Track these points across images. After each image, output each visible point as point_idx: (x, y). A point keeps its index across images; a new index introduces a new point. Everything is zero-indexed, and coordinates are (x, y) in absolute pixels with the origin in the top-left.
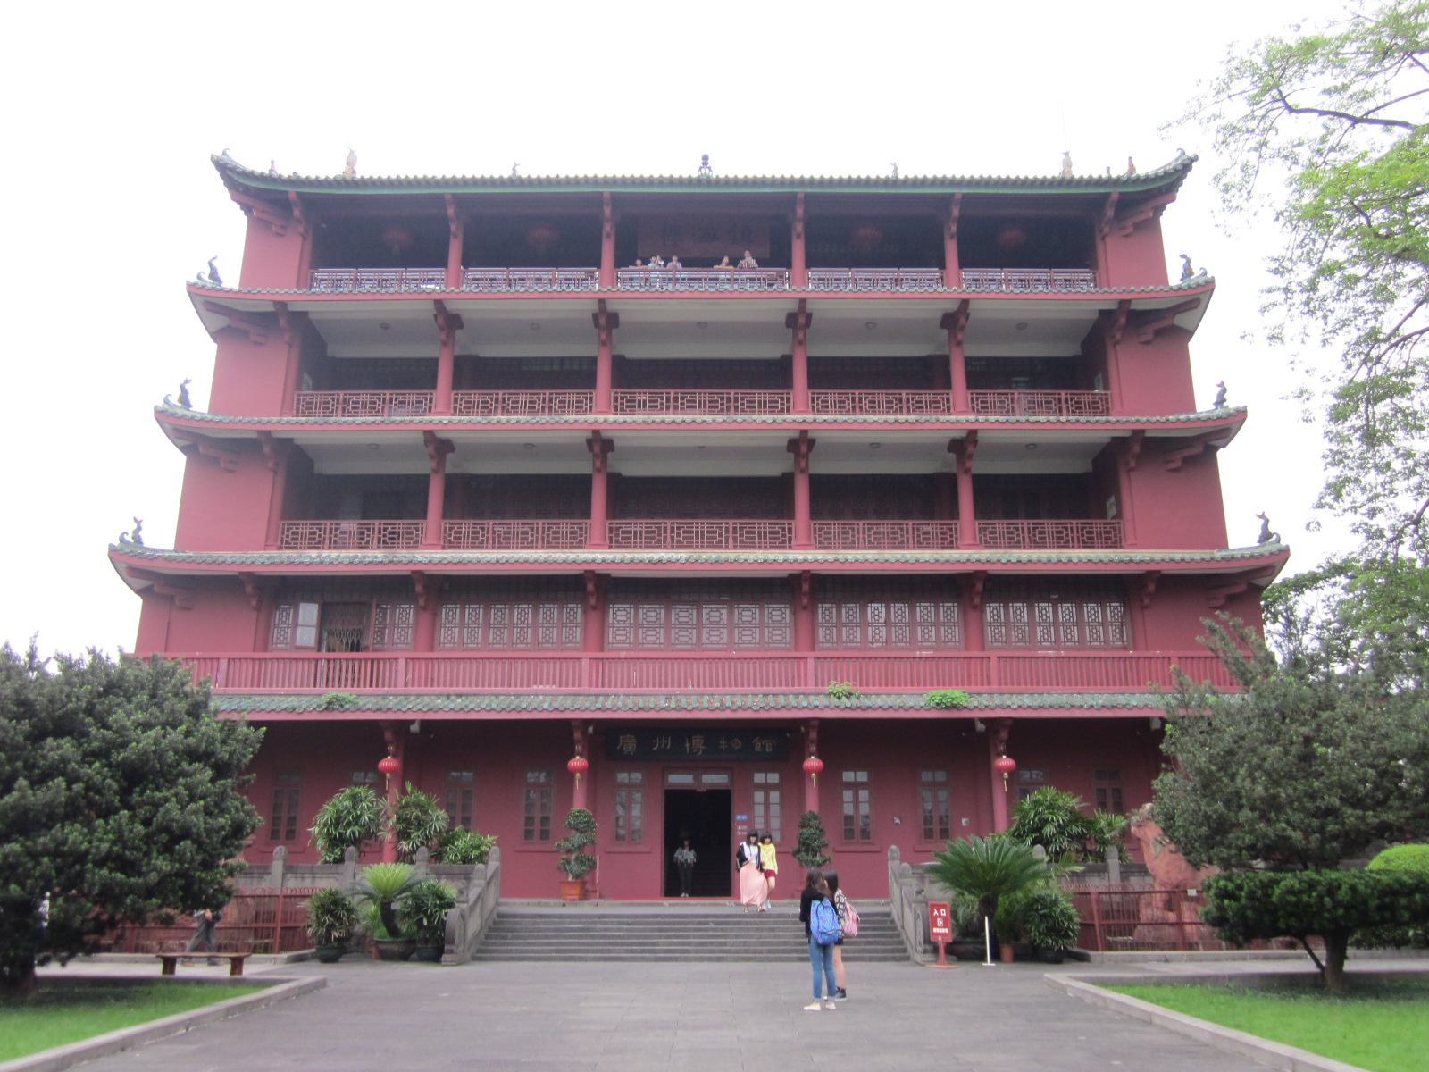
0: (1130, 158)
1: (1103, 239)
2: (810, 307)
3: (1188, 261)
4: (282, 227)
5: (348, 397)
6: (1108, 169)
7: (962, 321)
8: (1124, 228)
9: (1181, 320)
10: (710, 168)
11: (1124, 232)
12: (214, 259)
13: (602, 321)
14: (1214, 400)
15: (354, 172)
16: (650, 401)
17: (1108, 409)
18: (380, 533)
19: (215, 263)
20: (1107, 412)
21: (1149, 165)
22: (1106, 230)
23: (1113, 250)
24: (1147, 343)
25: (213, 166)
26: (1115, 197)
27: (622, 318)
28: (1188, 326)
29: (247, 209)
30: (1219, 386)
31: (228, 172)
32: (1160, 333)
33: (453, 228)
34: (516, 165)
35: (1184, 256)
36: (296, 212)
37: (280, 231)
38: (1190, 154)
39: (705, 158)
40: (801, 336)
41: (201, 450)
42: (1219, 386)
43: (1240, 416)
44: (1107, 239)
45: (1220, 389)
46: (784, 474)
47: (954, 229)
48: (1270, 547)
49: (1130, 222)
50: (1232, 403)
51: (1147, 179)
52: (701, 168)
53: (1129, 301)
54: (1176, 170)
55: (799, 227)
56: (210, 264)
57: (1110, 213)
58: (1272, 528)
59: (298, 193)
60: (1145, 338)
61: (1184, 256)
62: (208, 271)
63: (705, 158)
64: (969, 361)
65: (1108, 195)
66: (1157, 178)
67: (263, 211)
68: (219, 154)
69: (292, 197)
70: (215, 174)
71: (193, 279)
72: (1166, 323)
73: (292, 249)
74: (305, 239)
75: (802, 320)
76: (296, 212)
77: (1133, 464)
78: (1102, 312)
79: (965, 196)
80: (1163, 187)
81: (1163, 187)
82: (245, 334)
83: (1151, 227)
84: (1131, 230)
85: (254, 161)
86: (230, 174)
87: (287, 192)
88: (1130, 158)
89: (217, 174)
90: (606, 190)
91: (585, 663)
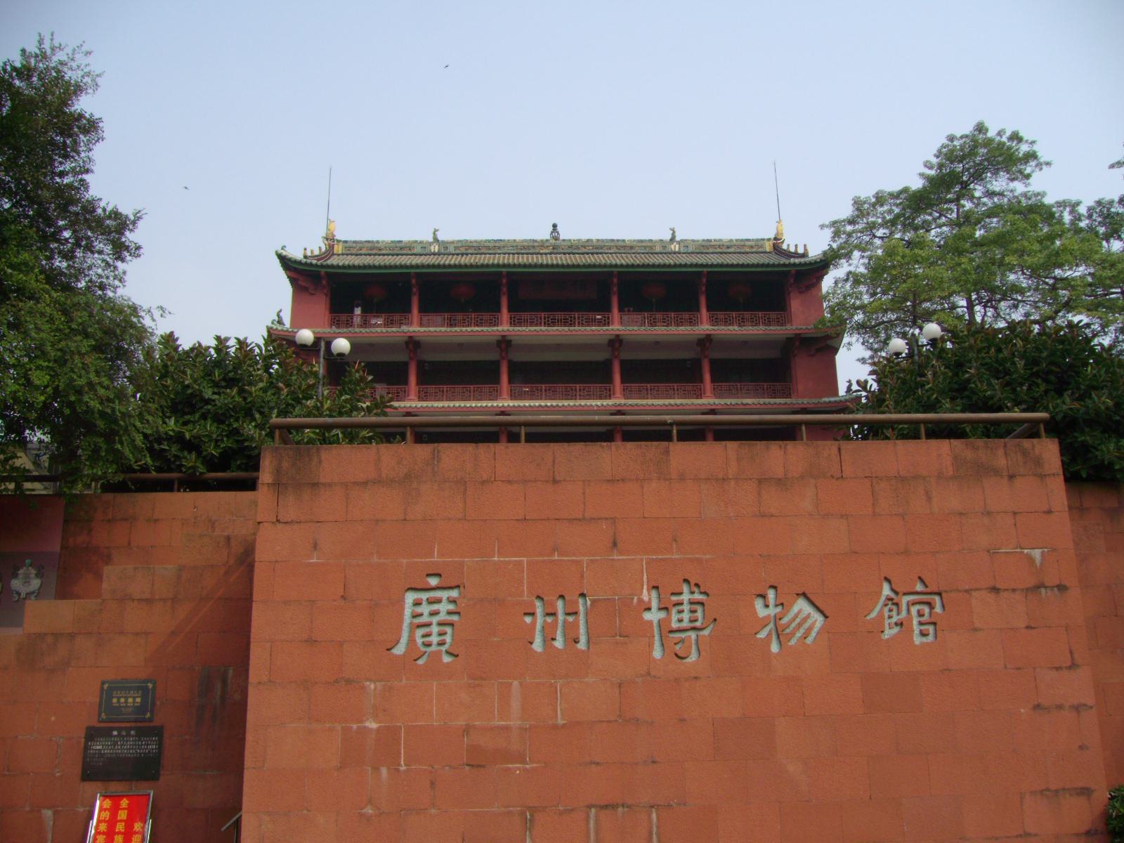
0: (805, 245)
1: (789, 294)
2: (621, 337)
6: (796, 246)
7: (708, 344)
10: (558, 232)
12: (280, 311)
13: (503, 346)
14: (846, 390)
16: (531, 391)
17: (790, 393)
19: (281, 314)
20: (789, 396)
22: (790, 289)
24: (812, 356)
25: (276, 257)
26: (793, 272)
27: (513, 343)
28: (837, 347)
29: (293, 281)
30: (848, 382)
31: (285, 260)
32: (818, 350)
33: (414, 290)
34: (436, 231)
36: (324, 282)
39: (555, 226)
40: (616, 353)
42: (848, 382)
44: (791, 295)
45: (848, 384)
47: (704, 289)
51: (811, 263)
52: (552, 232)
53: (800, 334)
55: (615, 289)
56: (278, 315)
57: (792, 281)
62: (277, 319)
63: (555, 226)
64: (713, 363)
66: (816, 262)
68: (280, 251)
70: (277, 262)
71: (270, 325)
73: (320, 306)
74: (327, 296)
75: (617, 345)
78: (788, 339)
79: (708, 272)
85: (296, 253)
86: (286, 262)
87: (320, 271)
88: (805, 245)
89: (278, 261)
90: (504, 270)
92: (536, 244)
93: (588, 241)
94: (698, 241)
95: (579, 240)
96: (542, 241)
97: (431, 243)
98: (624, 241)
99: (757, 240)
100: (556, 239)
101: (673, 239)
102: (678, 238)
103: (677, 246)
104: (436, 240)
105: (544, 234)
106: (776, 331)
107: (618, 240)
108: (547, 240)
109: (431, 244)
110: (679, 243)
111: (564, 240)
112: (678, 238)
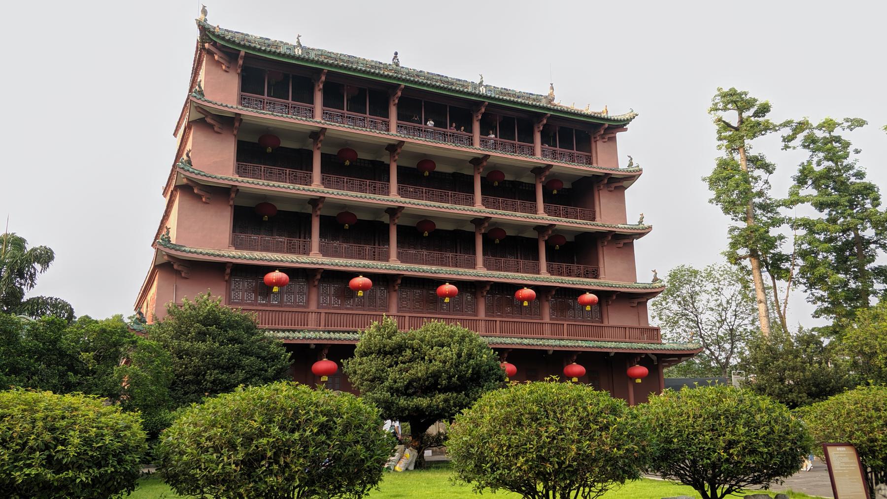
1: (596, 142)
3: (631, 159)
4: (228, 67)
5: (240, 165)
8: (604, 138)
9: (625, 183)
11: (605, 140)
15: (206, 20)
18: (287, 245)
21: (615, 113)
23: (600, 149)
25: (196, 26)
26: (606, 126)
32: (616, 188)
34: (299, 36)
35: (629, 157)
37: (227, 70)
38: (635, 112)
39: (396, 54)
41: (196, 191)
43: (650, 228)
46: (455, 230)
48: (659, 285)
49: (607, 137)
50: (646, 223)
52: (394, 59)
53: (611, 174)
54: (627, 119)
57: (602, 132)
58: (658, 277)
59: (246, 52)
60: (611, 189)
61: (629, 157)
65: (603, 124)
67: (221, 57)
69: (242, 53)
72: (620, 184)
76: (241, 62)
77: (606, 243)
80: (620, 125)
81: (620, 125)
82: (210, 127)
83: (613, 139)
84: (607, 140)
91: (407, 318)
92: (381, 66)
93: (421, 71)
94: (498, 88)
95: (414, 70)
96: (386, 64)
97: (294, 46)
98: (447, 77)
99: (537, 95)
100: (397, 65)
101: (481, 84)
102: (484, 84)
103: (484, 89)
104: (300, 45)
105: (387, 59)
106: (581, 168)
107: (443, 76)
108: (390, 65)
109: (294, 47)
110: (486, 86)
111: (403, 67)
112: (484, 84)
